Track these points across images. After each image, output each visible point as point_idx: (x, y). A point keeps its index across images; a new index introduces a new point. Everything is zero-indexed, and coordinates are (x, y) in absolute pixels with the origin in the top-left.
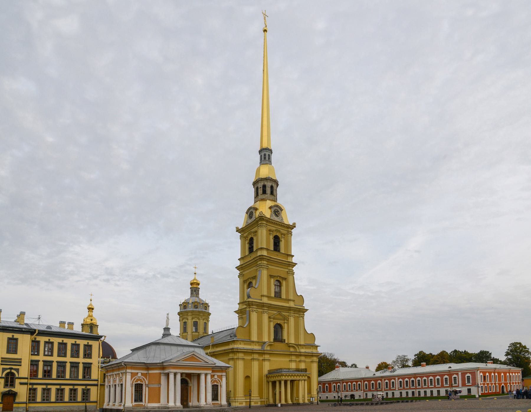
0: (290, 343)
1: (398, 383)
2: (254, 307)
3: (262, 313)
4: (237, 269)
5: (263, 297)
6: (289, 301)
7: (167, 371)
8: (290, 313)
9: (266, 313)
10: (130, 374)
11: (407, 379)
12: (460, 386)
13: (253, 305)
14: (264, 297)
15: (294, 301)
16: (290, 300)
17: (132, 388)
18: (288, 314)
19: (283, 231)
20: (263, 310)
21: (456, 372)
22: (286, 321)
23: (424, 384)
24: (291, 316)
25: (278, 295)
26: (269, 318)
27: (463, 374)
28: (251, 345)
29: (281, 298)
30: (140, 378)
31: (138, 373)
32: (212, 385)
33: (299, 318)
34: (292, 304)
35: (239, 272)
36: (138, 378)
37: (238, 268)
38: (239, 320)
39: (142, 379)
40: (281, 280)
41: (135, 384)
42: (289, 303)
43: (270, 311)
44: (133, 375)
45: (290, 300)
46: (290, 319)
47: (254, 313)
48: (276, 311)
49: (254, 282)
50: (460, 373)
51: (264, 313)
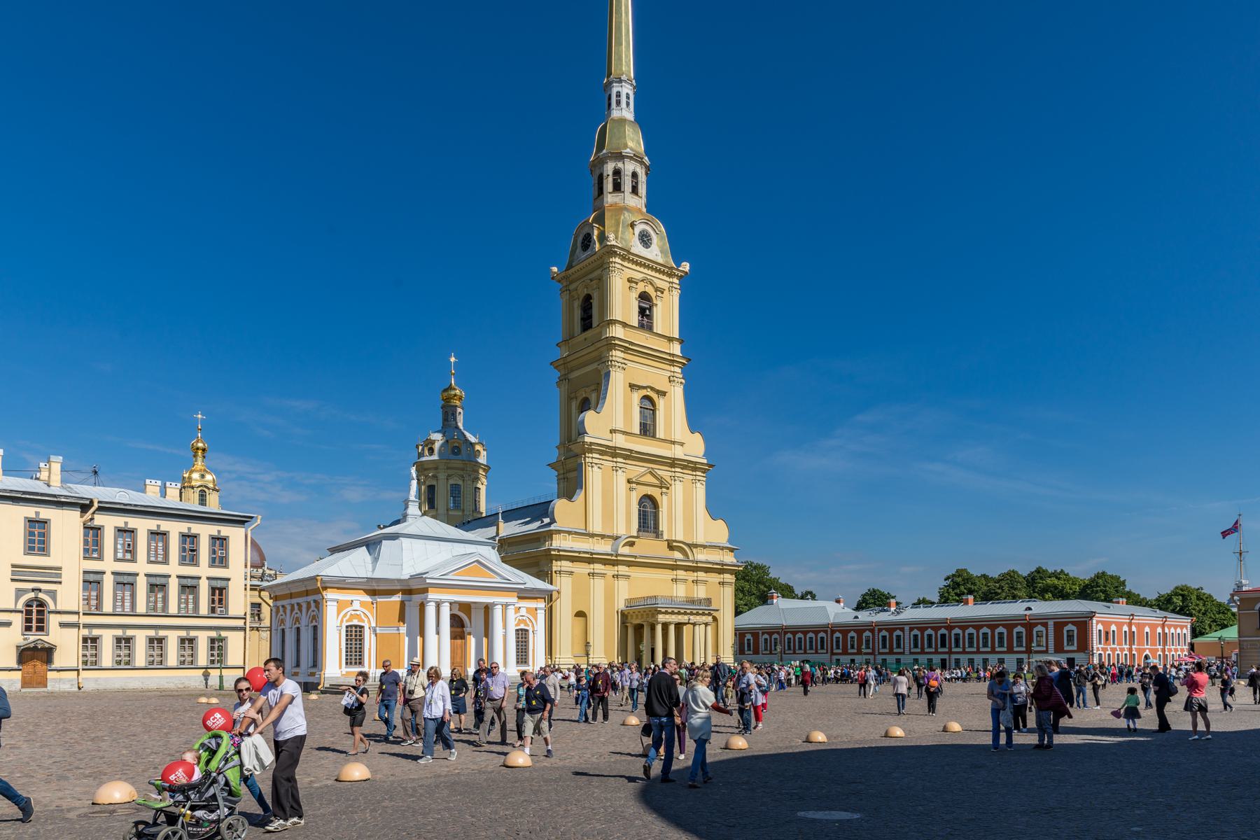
0: (674, 539)
1: (910, 640)
2: (595, 455)
4: (555, 368)
5: (614, 434)
7: (417, 598)
10: (335, 603)
11: (930, 631)
12: (1049, 652)
13: (591, 451)
15: (682, 444)
16: (674, 443)
17: (340, 634)
18: (670, 474)
19: (659, 284)
21: (1043, 620)
22: (664, 490)
23: (969, 643)
25: (647, 430)
26: (629, 481)
27: (1059, 626)
29: (654, 436)
30: (358, 613)
31: (352, 601)
32: (517, 630)
34: (678, 452)
35: (559, 374)
36: (353, 613)
37: (557, 365)
38: (558, 484)
39: (362, 614)
40: (654, 396)
41: (347, 627)
42: (673, 449)
44: (341, 605)
45: (674, 442)
46: (673, 486)
47: (595, 468)
48: (643, 467)
49: (593, 397)
50: (1051, 623)
51: (617, 471)
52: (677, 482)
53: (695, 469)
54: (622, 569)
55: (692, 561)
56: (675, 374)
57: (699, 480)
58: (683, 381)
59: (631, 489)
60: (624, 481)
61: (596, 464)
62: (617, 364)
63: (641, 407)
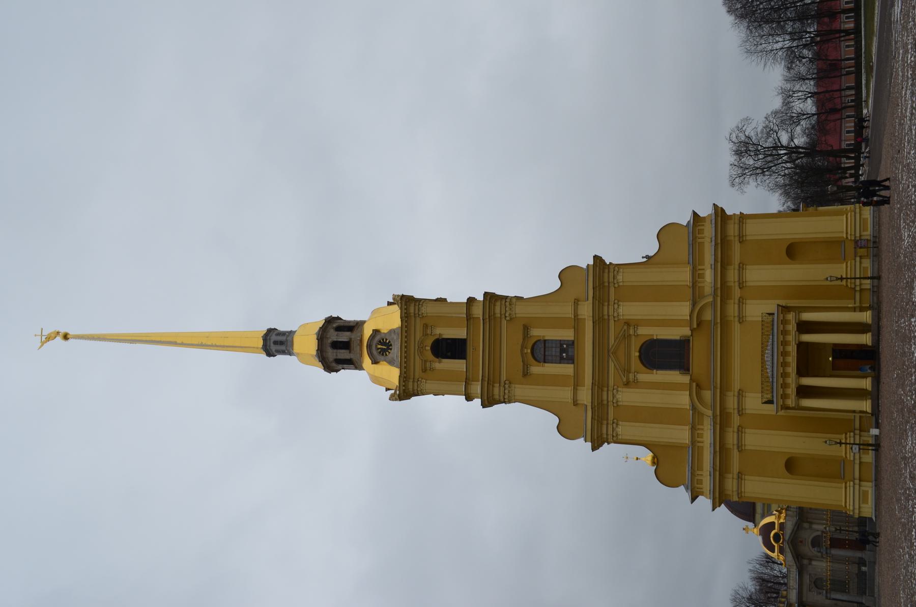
2: (604, 431)
3: (617, 406)
8: (609, 316)
9: (618, 396)
14: (578, 399)
15: (576, 302)
16: (576, 315)
18: (612, 323)
22: (632, 332)
24: (616, 314)
26: (627, 384)
29: (573, 342)
33: (619, 286)
34: (586, 311)
42: (583, 317)
43: (611, 383)
46: (625, 318)
47: (620, 430)
48: (608, 362)
54: (732, 403)
56: (503, 312)
57: (614, 279)
61: (613, 431)
63: (545, 362)
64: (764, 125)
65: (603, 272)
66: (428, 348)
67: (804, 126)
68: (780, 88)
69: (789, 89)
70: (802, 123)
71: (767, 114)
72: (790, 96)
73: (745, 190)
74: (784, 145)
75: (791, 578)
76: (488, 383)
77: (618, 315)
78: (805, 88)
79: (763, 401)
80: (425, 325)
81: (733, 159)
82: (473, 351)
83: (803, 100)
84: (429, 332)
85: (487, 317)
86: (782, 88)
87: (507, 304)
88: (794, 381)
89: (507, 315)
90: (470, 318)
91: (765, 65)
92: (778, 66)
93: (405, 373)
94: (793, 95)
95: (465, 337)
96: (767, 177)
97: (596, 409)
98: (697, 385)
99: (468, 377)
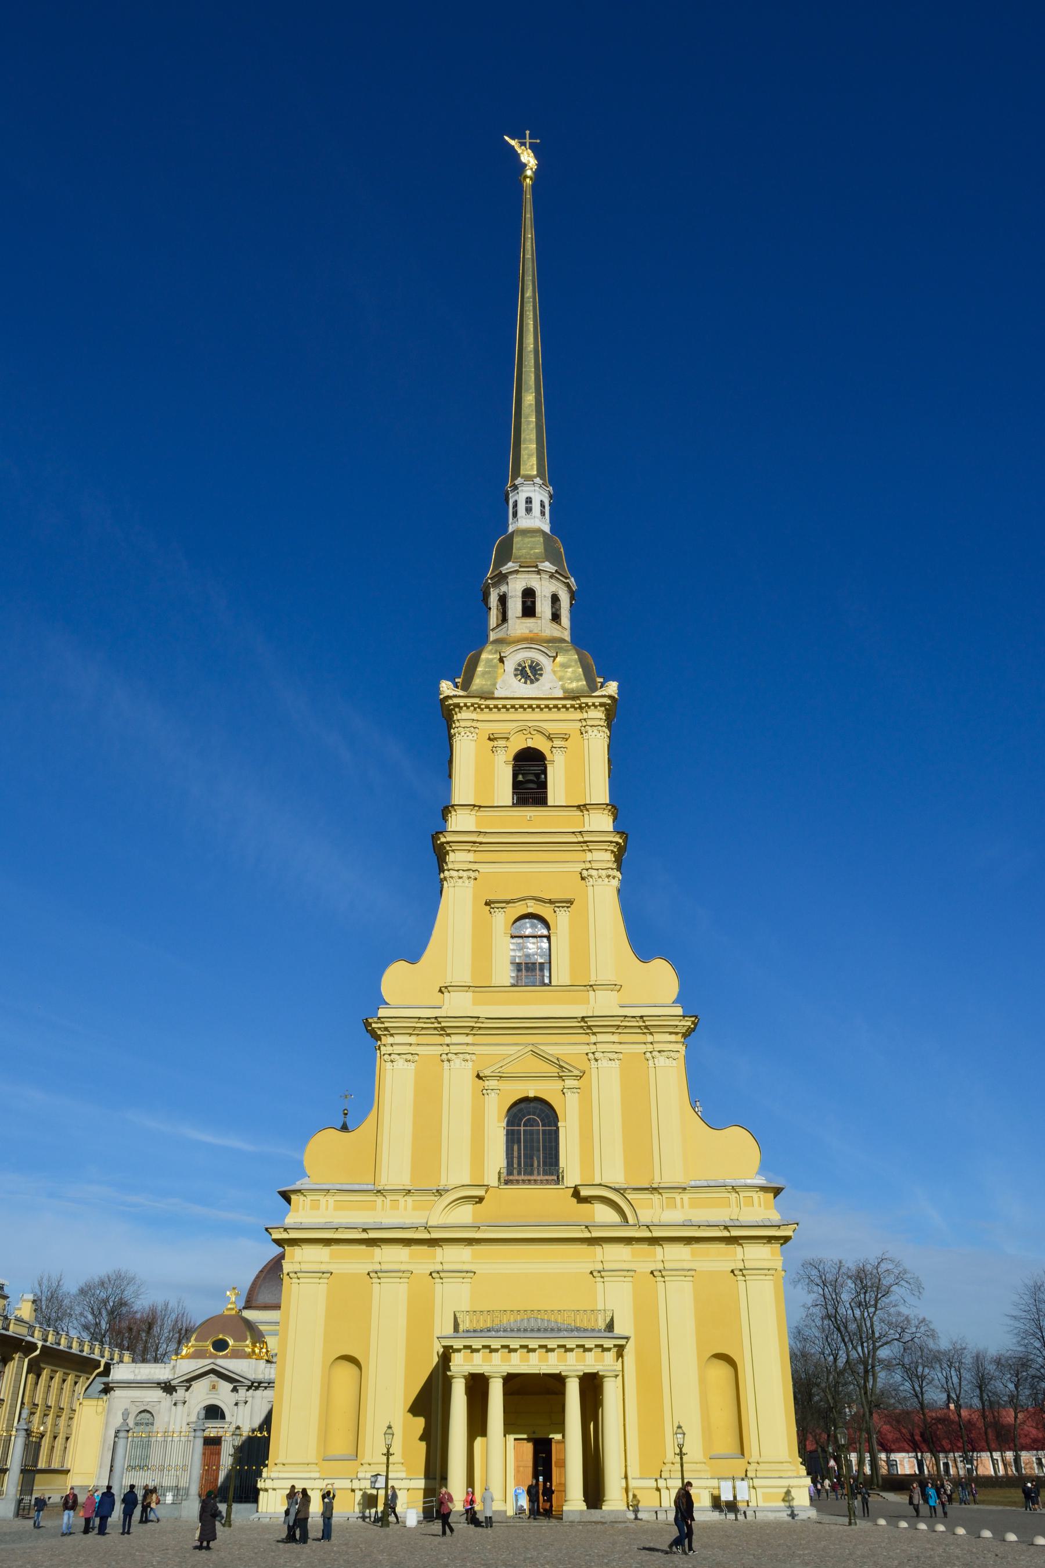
2: (398, 1039)
5: (446, 994)
6: (591, 993)
15: (616, 987)
18: (586, 1049)
20: (446, 1049)
22: (570, 1083)
24: (598, 1055)
28: (374, 1209)
34: (603, 1004)
46: (594, 1071)
47: (400, 1063)
52: (604, 1063)
53: (647, 1030)
55: (638, 1225)
56: (595, 865)
58: (618, 874)
59: (484, 1091)
60: (470, 1076)
62: (454, 874)
64: (912, 1316)
65: (671, 1033)
66: (531, 744)
67: (901, 1388)
68: (964, 1346)
69: (963, 1361)
70: (907, 1383)
71: (930, 1322)
72: (951, 1363)
73: (799, 1286)
74: (878, 1352)
75: (153, 1371)
76: (474, 843)
77: (596, 1060)
78: (966, 1388)
79: (458, 1315)
80: (567, 737)
81: (851, 1264)
82: (527, 816)
83: (945, 1386)
84: (557, 743)
85: (586, 839)
86: (965, 1349)
87: (610, 872)
88: (494, 1369)
89: (591, 872)
90: (582, 811)
91: (1015, 1318)
92: (1014, 1341)
93: (487, 707)
94: (953, 1369)
95: (550, 802)
96: (819, 1323)
97: (436, 1025)
98: (481, 1199)
99: (482, 809)
